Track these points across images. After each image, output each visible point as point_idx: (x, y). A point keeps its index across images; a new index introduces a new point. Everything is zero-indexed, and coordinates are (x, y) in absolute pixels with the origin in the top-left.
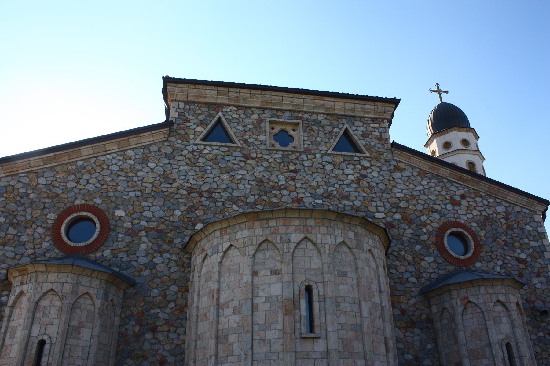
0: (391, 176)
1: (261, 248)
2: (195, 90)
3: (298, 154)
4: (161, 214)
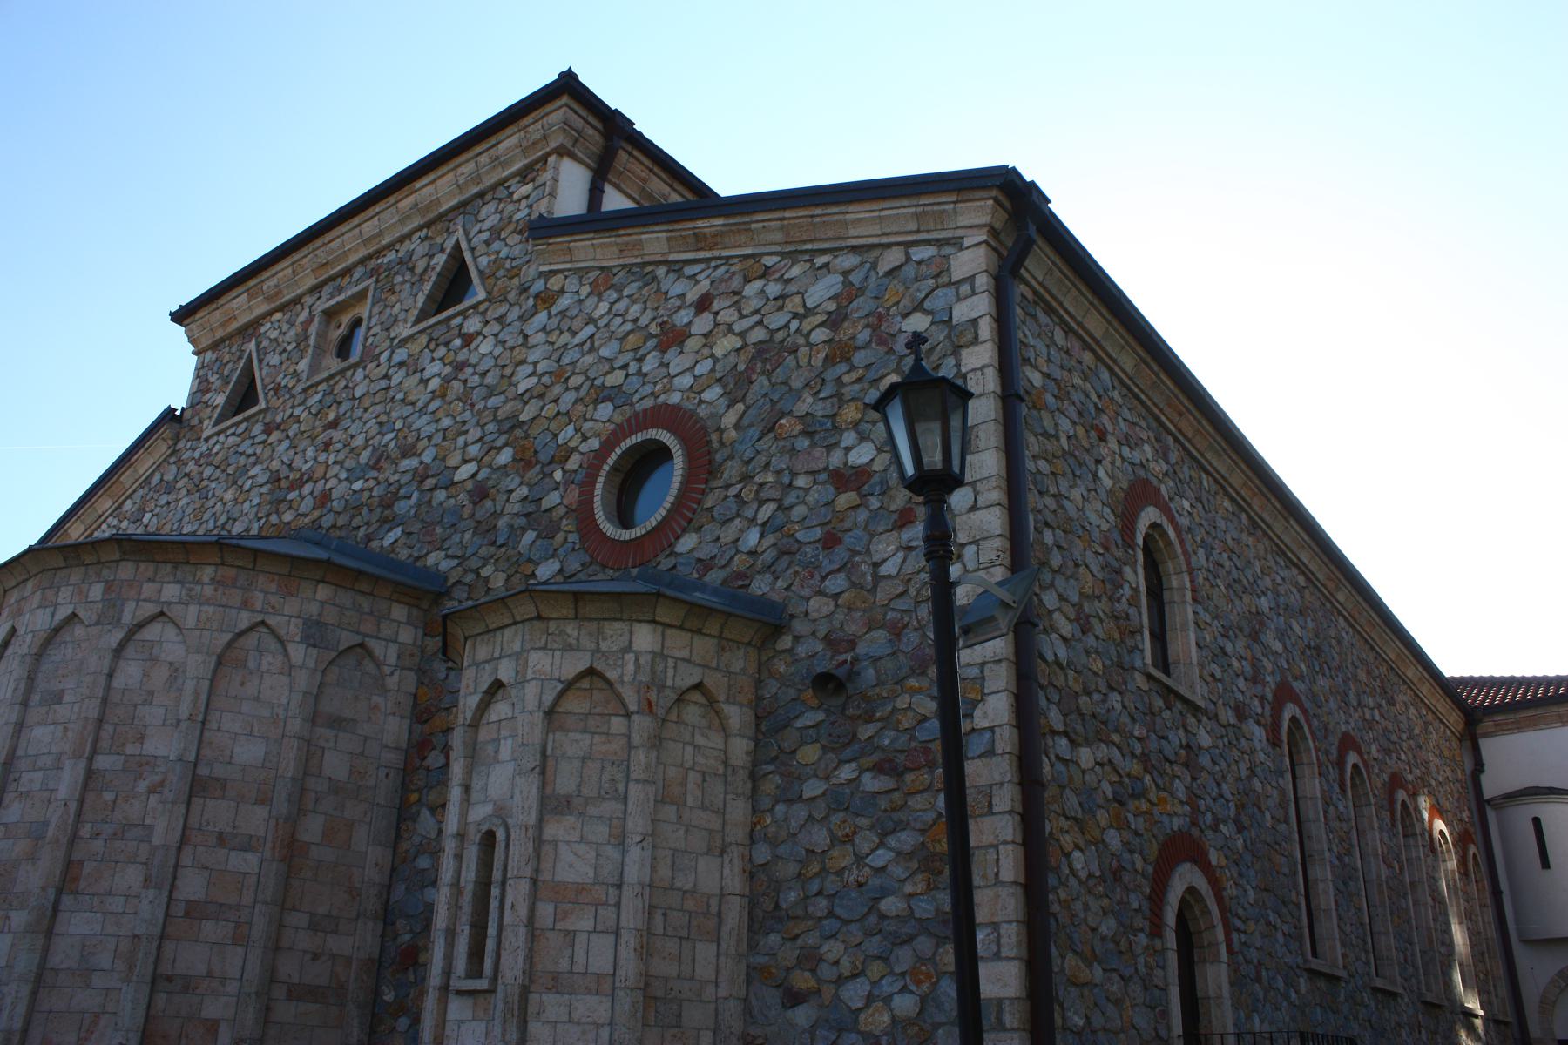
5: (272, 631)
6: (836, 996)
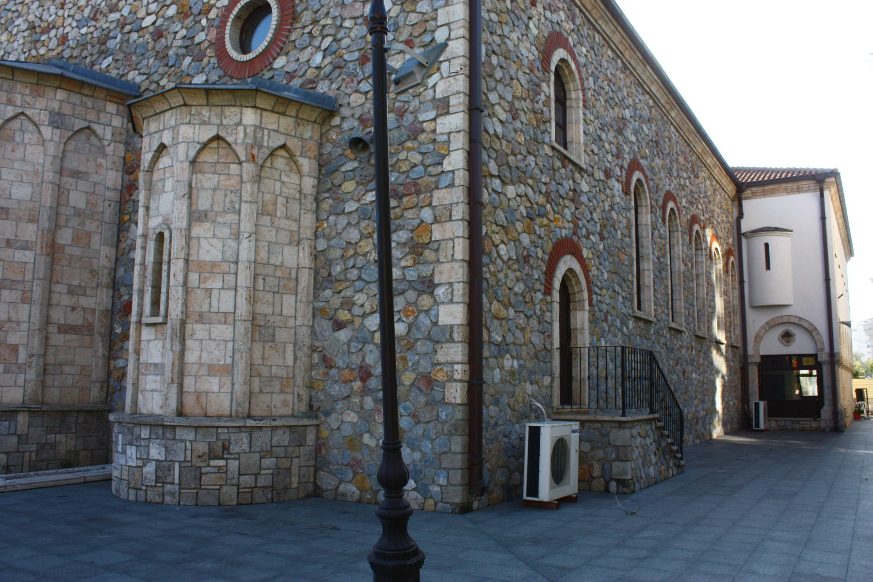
5: (29, 119)
6: (362, 324)
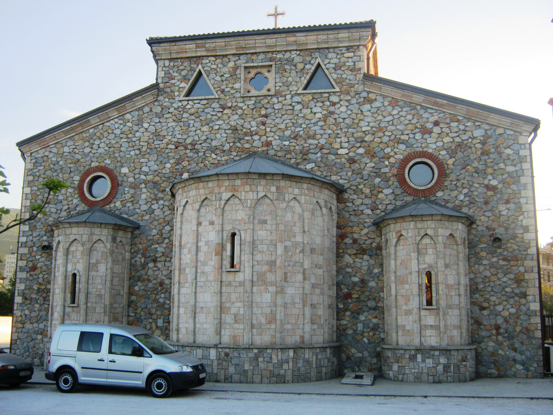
0: (359, 109)
1: (204, 204)
2: (176, 47)
3: (270, 97)
4: (156, 167)
6: (494, 308)
